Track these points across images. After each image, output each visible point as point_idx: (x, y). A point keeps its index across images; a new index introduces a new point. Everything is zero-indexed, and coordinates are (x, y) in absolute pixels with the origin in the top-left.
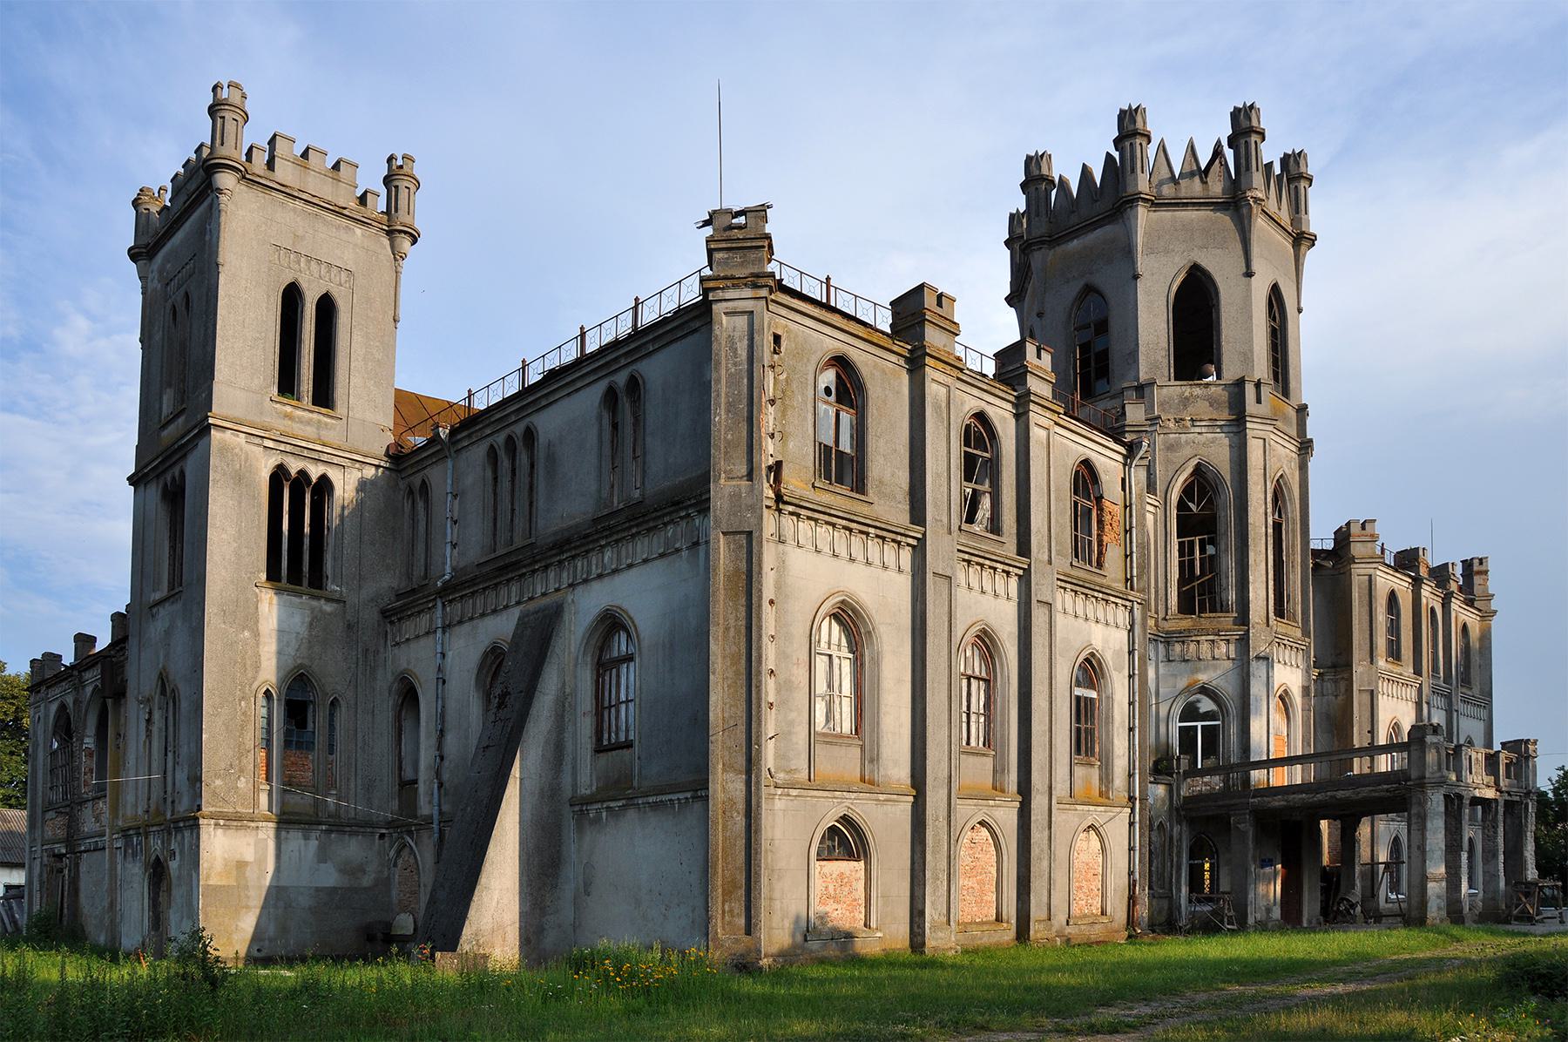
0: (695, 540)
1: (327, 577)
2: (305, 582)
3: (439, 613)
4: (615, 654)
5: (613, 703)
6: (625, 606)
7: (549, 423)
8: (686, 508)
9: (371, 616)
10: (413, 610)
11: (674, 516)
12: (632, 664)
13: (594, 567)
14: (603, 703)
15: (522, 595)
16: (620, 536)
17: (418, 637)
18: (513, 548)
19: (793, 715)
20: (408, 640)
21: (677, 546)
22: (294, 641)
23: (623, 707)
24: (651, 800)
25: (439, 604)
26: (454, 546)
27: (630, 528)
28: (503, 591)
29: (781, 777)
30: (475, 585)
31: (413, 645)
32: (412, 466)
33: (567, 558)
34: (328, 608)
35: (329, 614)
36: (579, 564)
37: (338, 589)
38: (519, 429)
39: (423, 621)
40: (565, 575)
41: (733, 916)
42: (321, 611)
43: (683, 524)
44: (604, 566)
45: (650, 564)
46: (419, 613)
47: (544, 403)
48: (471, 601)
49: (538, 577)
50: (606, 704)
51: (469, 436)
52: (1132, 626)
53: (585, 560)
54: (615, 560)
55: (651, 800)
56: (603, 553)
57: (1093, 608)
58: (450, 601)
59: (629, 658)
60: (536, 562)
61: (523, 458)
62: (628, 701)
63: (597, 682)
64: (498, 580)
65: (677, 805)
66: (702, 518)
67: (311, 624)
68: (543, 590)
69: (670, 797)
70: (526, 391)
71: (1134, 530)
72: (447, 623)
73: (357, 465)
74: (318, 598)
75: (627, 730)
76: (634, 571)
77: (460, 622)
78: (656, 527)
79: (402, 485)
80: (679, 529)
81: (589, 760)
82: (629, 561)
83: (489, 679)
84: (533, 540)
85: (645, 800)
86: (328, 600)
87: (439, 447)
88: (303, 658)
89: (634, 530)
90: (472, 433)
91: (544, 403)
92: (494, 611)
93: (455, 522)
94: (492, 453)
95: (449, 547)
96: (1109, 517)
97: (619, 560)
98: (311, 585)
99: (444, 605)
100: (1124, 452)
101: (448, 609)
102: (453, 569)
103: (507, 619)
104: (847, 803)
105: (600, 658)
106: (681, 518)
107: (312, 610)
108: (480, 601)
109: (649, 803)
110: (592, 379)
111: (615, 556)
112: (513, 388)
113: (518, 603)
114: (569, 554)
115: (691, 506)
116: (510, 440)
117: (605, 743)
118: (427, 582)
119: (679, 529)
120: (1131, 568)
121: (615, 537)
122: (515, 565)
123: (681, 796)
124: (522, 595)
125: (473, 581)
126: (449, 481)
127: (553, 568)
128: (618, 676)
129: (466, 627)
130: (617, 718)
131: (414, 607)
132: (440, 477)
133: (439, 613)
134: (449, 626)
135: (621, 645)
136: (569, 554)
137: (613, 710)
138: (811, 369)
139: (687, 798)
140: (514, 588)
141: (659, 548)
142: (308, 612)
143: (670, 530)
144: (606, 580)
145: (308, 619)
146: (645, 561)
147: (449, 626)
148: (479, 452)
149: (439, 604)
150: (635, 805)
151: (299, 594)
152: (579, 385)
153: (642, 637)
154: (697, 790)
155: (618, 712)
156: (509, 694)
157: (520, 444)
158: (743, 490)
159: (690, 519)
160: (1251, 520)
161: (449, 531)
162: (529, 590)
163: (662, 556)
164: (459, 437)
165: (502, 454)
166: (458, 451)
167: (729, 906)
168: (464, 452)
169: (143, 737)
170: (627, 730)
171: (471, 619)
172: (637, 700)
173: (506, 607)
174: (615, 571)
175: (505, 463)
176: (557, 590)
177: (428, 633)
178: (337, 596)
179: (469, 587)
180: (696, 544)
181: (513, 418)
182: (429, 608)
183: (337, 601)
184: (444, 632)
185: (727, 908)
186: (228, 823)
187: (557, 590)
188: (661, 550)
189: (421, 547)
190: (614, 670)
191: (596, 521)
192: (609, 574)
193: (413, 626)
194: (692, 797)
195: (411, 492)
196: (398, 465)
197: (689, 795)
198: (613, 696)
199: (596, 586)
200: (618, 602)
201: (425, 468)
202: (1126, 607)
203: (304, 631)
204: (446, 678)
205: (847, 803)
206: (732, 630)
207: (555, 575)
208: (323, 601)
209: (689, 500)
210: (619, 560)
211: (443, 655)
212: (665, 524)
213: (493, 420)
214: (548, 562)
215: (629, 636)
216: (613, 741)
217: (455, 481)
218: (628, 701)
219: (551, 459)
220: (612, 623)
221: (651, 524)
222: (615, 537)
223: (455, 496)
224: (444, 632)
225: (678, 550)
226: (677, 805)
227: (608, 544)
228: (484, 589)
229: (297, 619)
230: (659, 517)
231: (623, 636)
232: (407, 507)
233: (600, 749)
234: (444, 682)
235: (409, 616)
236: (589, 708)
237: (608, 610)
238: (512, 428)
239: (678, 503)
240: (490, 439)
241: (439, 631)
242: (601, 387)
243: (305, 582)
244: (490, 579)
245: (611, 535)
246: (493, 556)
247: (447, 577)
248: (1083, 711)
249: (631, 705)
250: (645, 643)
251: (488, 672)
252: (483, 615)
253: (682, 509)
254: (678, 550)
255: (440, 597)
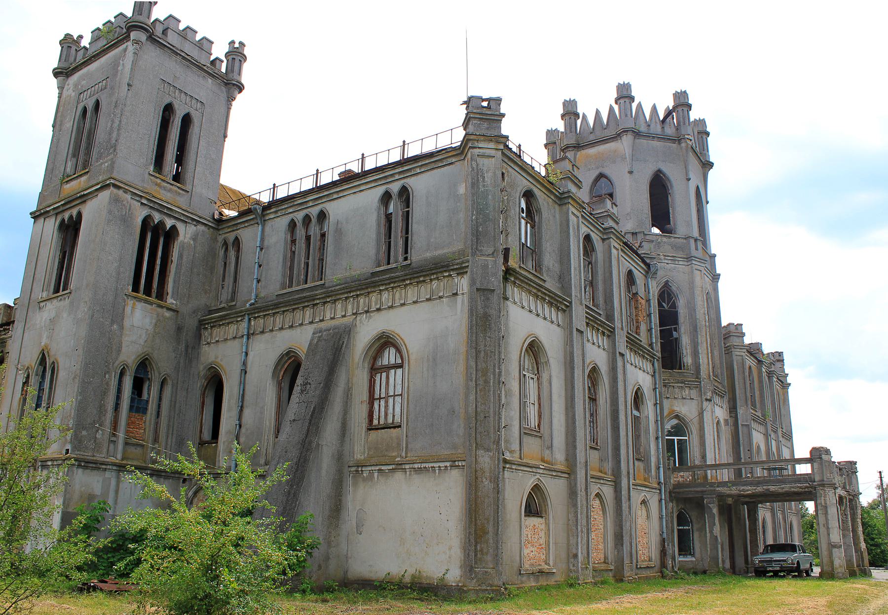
0: (455, 292)
1: (168, 293)
2: (154, 294)
3: (245, 324)
4: (385, 362)
5: (382, 396)
6: (397, 331)
7: (337, 209)
8: (449, 271)
9: (191, 323)
10: (224, 322)
11: (439, 275)
12: (399, 371)
13: (373, 304)
14: (374, 396)
15: (314, 317)
16: (396, 285)
17: (226, 340)
18: (306, 286)
19: (513, 413)
20: (218, 341)
21: (441, 294)
22: (144, 335)
23: (391, 400)
24: (416, 466)
25: (246, 318)
26: (258, 281)
27: (404, 280)
28: (298, 315)
29: (508, 456)
30: (277, 308)
31: (221, 345)
32: (229, 227)
33: (353, 296)
34: (168, 314)
35: (167, 319)
36: (362, 301)
37: (174, 302)
38: (314, 212)
39: (233, 328)
40: (350, 307)
41: (482, 554)
42: (163, 316)
43: (446, 279)
44: (381, 303)
45: (418, 305)
46: (228, 323)
47: (335, 196)
48: (272, 318)
49: (328, 306)
50: (377, 396)
51: (276, 212)
52: (654, 372)
53: (367, 299)
54: (390, 300)
55: (416, 466)
56: (381, 294)
57: (638, 360)
58: (255, 318)
59: (401, 366)
60: (329, 297)
61: (314, 230)
62: (394, 396)
63: (370, 381)
64: (296, 306)
65: (437, 471)
66: (459, 278)
67: (156, 325)
68: (332, 316)
69: (427, 465)
70: (318, 189)
71: (652, 315)
72: (252, 332)
73: (195, 223)
74: (161, 307)
75: (394, 416)
76: (405, 307)
77: (262, 332)
78: (424, 281)
79: (220, 239)
80: (442, 284)
81: (363, 435)
82: (402, 302)
83: (282, 373)
84: (322, 282)
85: (411, 466)
86: (169, 309)
87: (254, 216)
88: (149, 347)
89: (408, 282)
90: (279, 210)
91: (335, 196)
92: (291, 327)
93: (260, 266)
94: (292, 225)
95: (255, 281)
96: (640, 306)
97: (394, 300)
98: (157, 297)
99: (250, 319)
100: (646, 269)
101: (253, 323)
102: (257, 296)
103: (301, 333)
104: (538, 476)
105: (373, 365)
106: (444, 277)
107: (158, 315)
108: (279, 319)
109: (415, 468)
110: (373, 185)
111: (391, 297)
112: (308, 185)
113: (311, 323)
114: (355, 293)
115: (453, 270)
116: (307, 219)
117: (375, 422)
118: (234, 303)
119: (442, 284)
120: (651, 337)
121: (392, 285)
122: (312, 298)
123: (442, 464)
124: (314, 317)
125: (276, 306)
126: (259, 239)
127: (341, 301)
128: (388, 378)
129: (267, 336)
130: (386, 406)
131: (225, 319)
132: (249, 236)
133: (245, 324)
134: (253, 334)
135: (390, 357)
136: (355, 293)
137: (383, 402)
138: (518, 195)
139: (446, 467)
140: (308, 312)
141: (427, 295)
142: (155, 316)
143: (435, 283)
144: (383, 312)
145: (154, 321)
146: (415, 302)
147: (253, 334)
148: (284, 222)
149: (246, 318)
150: (403, 469)
151: (151, 304)
152: (362, 188)
153: (410, 353)
154: (455, 461)
155: (387, 402)
156: (310, 384)
157: (314, 220)
158: (490, 264)
159: (450, 279)
160: (698, 317)
161: (256, 270)
162: (320, 314)
163: (428, 300)
164: (268, 212)
165: (299, 225)
166: (265, 221)
167: (480, 547)
168: (269, 221)
169: (18, 395)
170: (394, 416)
171: (272, 331)
172: (406, 395)
173: (301, 325)
174: (391, 307)
175: (300, 232)
176: (344, 316)
177: (235, 338)
178: (174, 307)
179: (272, 309)
180: (456, 294)
181: (311, 204)
182: (237, 321)
183: (173, 310)
184: (248, 338)
185: (479, 548)
186: (86, 465)
187: (344, 316)
188: (428, 297)
189: (229, 280)
190: (384, 375)
191: (373, 274)
192: (385, 309)
193: (222, 333)
194: (451, 466)
195: (225, 244)
196: (218, 225)
197: (448, 464)
198: (383, 390)
199: (375, 316)
200: (392, 328)
201: (237, 230)
202: (651, 361)
203: (150, 328)
204: (248, 370)
205: (538, 476)
206: (482, 353)
207: (342, 307)
208: (165, 310)
209: (453, 265)
210: (394, 300)
211: (247, 354)
212: (431, 280)
213: (295, 203)
214: (338, 297)
215: (398, 350)
216: (382, 422)
217: (262, 240)
218: (394, 396)
219: (339, 231)
220: (385, 342)
221: (421, 279)
222: (392, 285)
223: (261, 249)
224: (248, 338)
225: (441, 297)
226: (437, 471)
227: (386, 289)
228: (284, 311)
229: (147, 320)
230: (428, 275)
231: (393, 351)
232: (222, 253)
233: (371, 428)
234: (246, 372)
235: (220, 325)
236: (365, 399)
237: (384, 332)
238: (309, 210)
239: (448, 266)
240: (291, 216)
241: (245, 337)
242: (380, 191)
243: (154, 294)
244: (290, 305)
245: (389, 284)
246: (290, 290)
247: (253, 301)
248: (636, 420)
249: (398, 399)
250: (413, 358)
251: (281, 368)
252: (281, 329)
253: (445, 271)
254: (441, 297)
255: (248, 314)
